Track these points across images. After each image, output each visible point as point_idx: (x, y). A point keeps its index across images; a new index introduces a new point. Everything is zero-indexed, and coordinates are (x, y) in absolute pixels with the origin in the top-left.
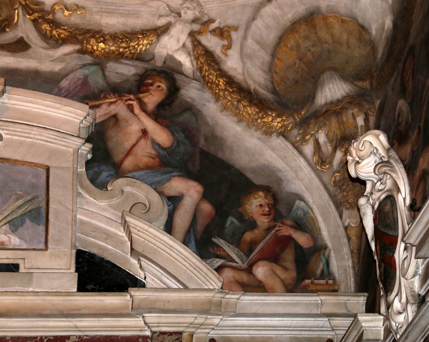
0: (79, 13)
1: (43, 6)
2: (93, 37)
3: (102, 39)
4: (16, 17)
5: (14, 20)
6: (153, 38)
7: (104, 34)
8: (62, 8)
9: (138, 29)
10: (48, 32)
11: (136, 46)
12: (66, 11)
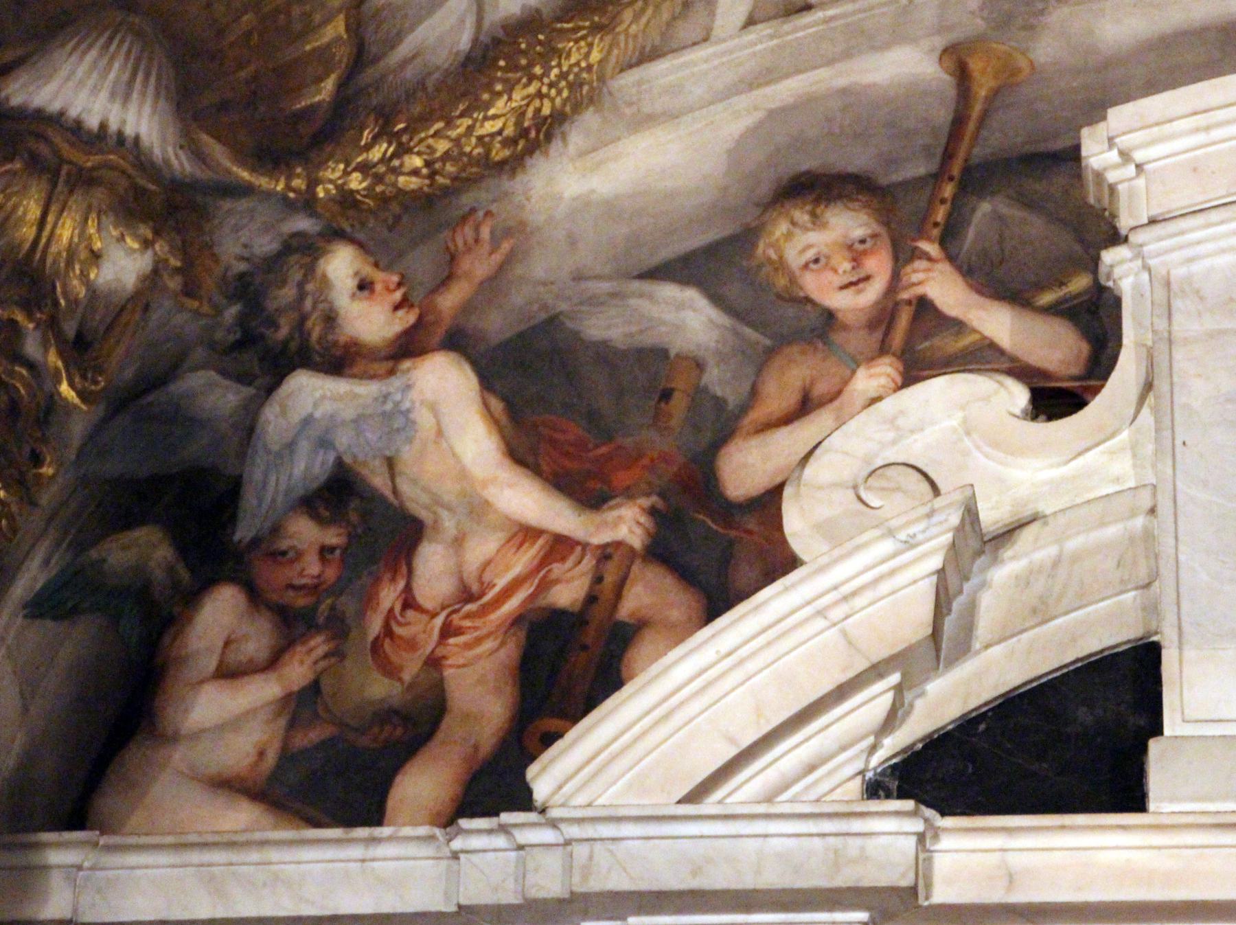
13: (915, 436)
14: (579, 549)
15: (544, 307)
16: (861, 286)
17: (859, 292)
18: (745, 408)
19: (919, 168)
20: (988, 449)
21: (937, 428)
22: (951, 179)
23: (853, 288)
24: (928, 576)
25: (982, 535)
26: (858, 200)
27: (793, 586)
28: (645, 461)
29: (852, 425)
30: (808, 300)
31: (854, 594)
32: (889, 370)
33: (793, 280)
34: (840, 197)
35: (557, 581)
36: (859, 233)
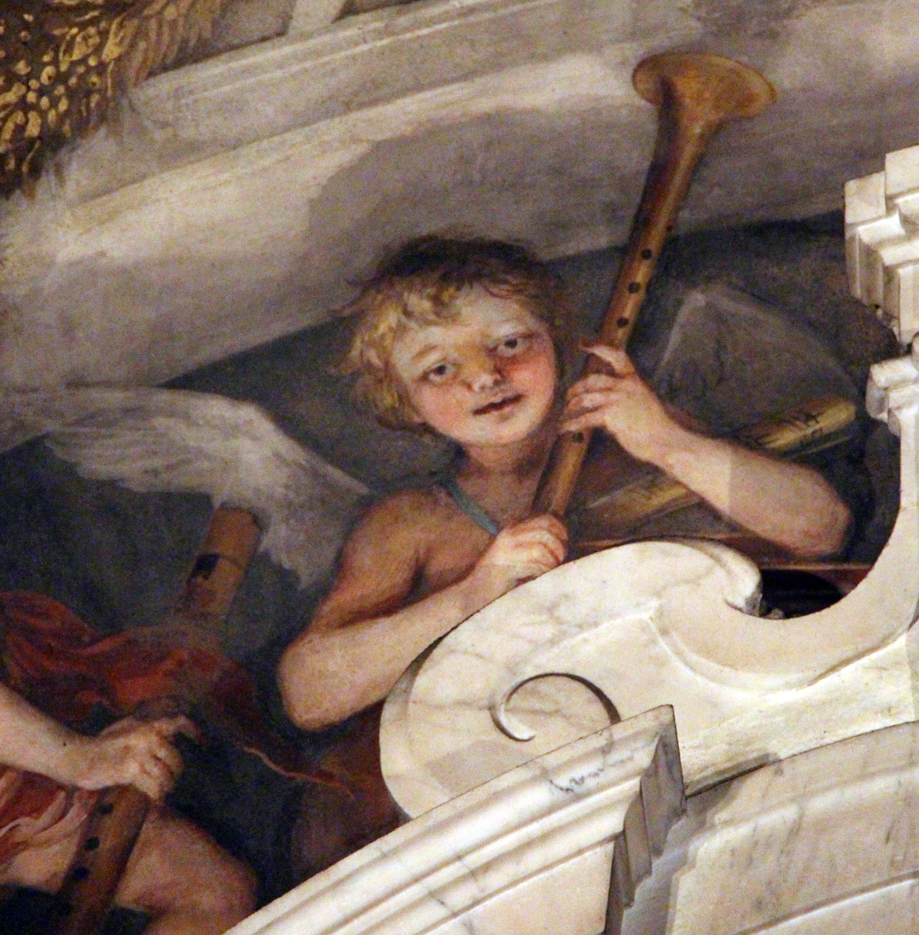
13: (585, 635)
14: (62, 795)
15: (21, 426)
16: (507, 410)
17: (504, 419)
18: (324, 590)
19: (601, 238)
20: (694, 658)
21: (618, 621)
22: (647, 255)
23: (495, 413)
24: (601, 843)
25: (685, 787)
26: (505, 282)
27: (395, 852)
28: (169, 665)
29: (490, 614)
30: (427, 429)
31: (487, 867)
32: (547, 537)
33: (404, 397)
34: (477, 277)
35: (25, 845)
36: (506, 330)
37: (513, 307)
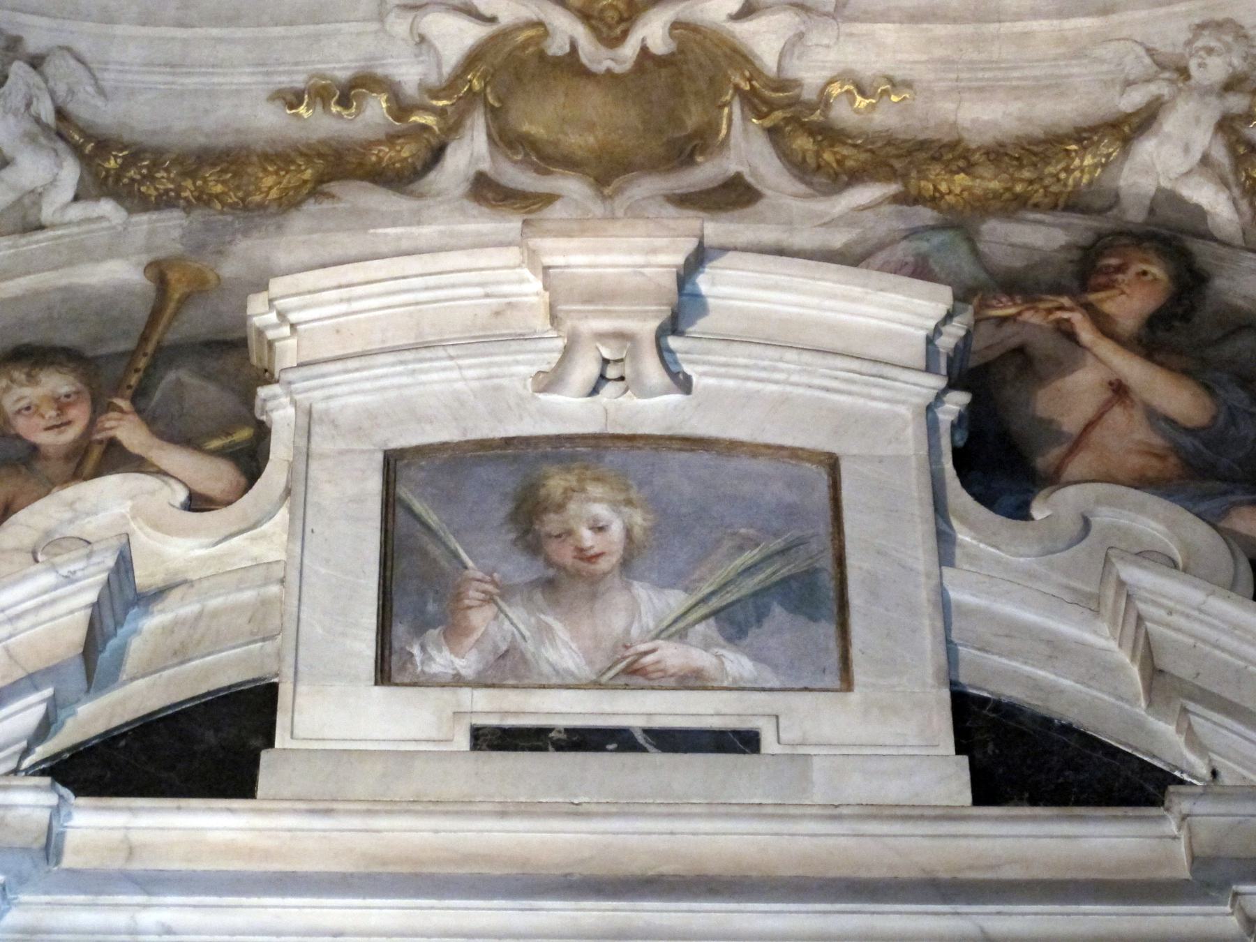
0: (894, 99)
1: (797, 91)
2: (934, 159)
3: (961, 163)
4: (724, 126)
5: (718, 132)
6: (1109, 148)
7: (968, 150)
8: (848, 92)
9: (1066, 127)
10: (811, 161)
11: (1063, 176)
12: (859, 98)
17: (60, 433)
30: (18, 437)
33: (7, 421)
34: (52, 363)
36: (65, 389)
37: (71, 378)
